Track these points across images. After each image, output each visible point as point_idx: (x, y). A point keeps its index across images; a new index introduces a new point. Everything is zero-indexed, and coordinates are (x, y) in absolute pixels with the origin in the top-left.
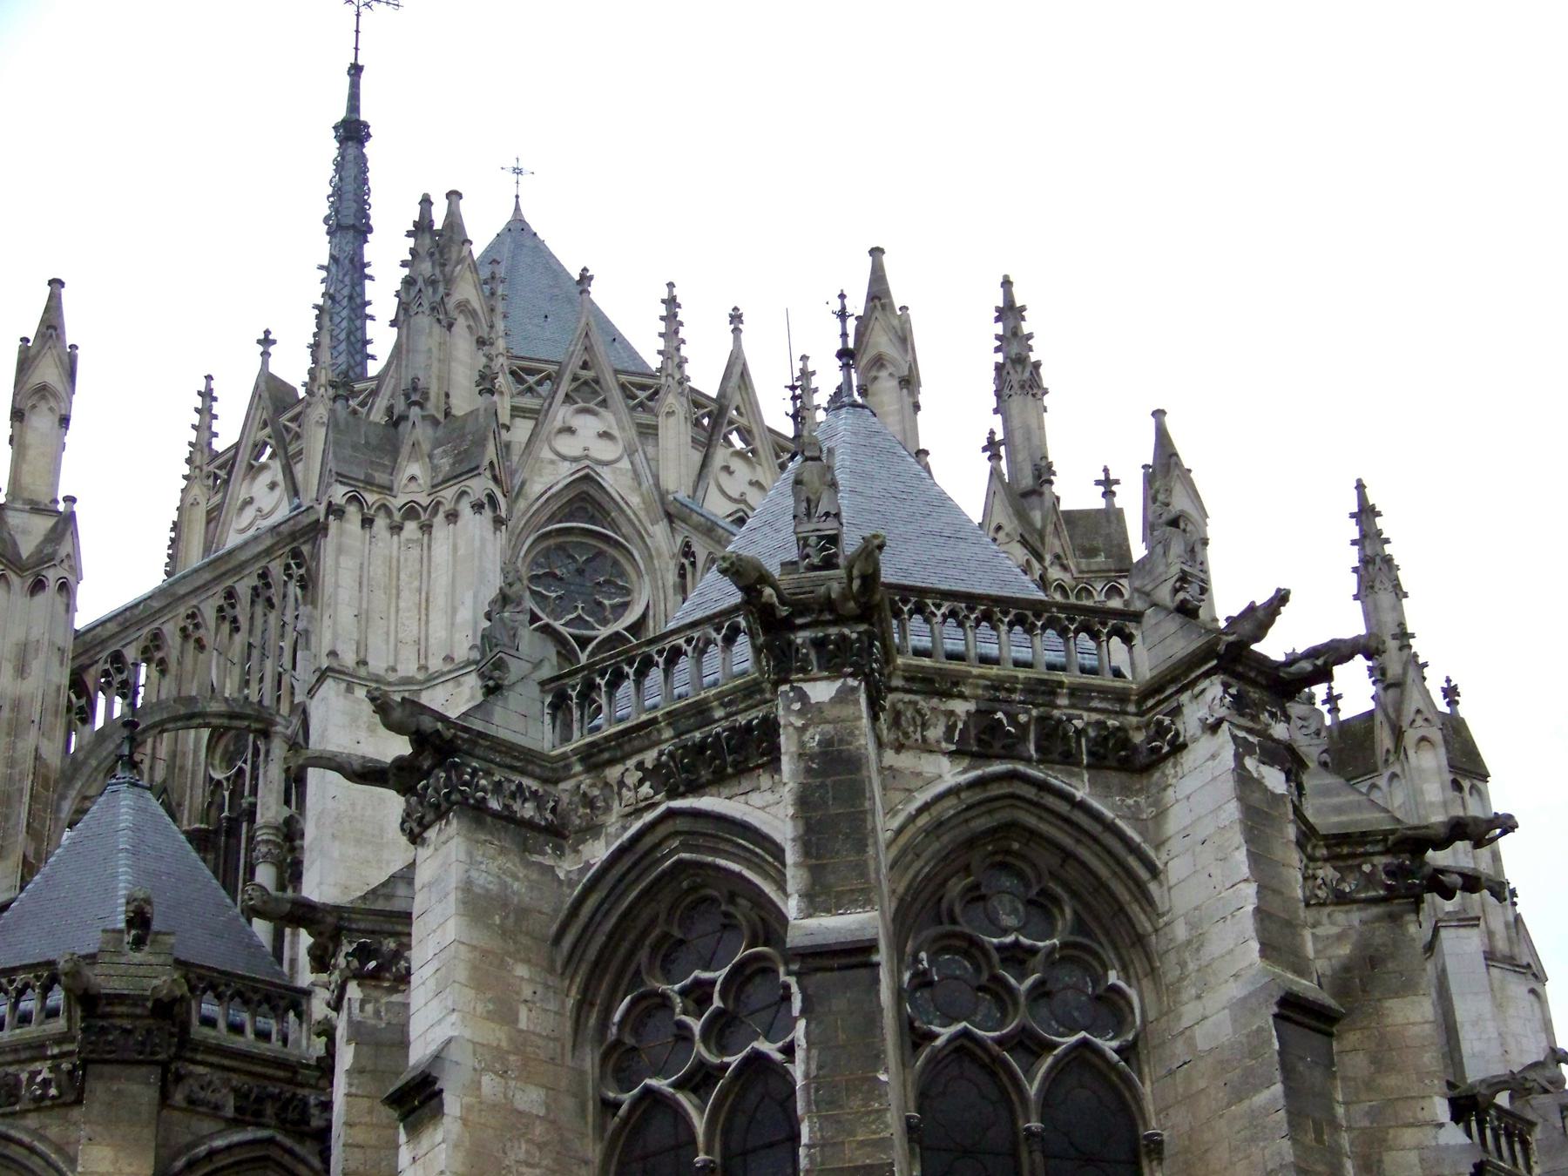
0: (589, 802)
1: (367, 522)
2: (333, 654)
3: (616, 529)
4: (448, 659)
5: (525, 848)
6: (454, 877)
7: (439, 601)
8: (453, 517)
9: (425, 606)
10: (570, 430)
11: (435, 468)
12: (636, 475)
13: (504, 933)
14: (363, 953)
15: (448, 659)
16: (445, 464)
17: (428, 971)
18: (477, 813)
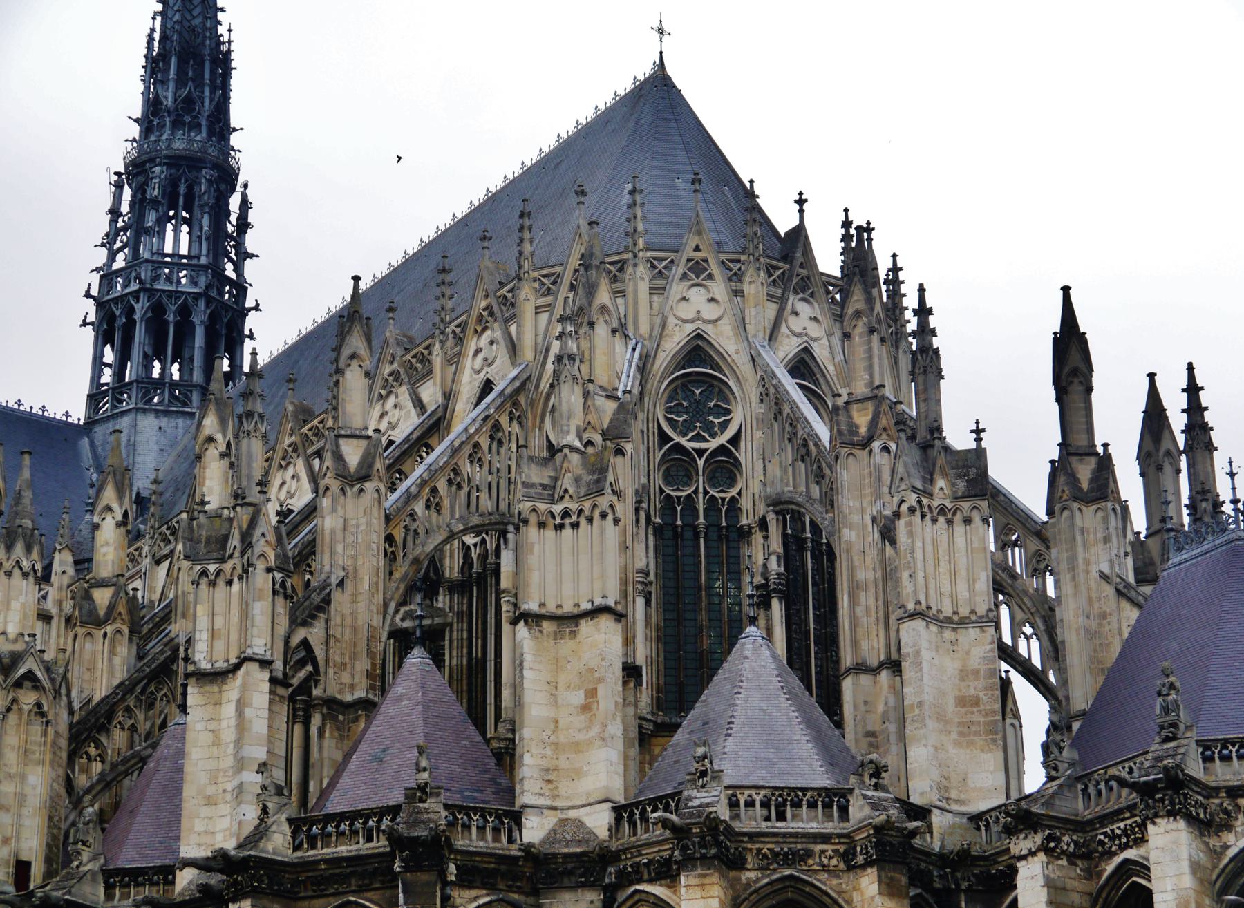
0: (1226, 812)
1: (923, 516)
2: (919, 603)
3: (816, 383)
5: (1202, 835)
6: (1185, 855)
7: (962, 573)
8: (967, 521)
9: (953, 574)
10: (796, 314)
11: (953, 485)
12: (831, 351)
13: (1201, 881)
14: (1050, 838)
15: (973, 612)
16: (961, 486)
17: (1169, 896)
18: (1192, 820)
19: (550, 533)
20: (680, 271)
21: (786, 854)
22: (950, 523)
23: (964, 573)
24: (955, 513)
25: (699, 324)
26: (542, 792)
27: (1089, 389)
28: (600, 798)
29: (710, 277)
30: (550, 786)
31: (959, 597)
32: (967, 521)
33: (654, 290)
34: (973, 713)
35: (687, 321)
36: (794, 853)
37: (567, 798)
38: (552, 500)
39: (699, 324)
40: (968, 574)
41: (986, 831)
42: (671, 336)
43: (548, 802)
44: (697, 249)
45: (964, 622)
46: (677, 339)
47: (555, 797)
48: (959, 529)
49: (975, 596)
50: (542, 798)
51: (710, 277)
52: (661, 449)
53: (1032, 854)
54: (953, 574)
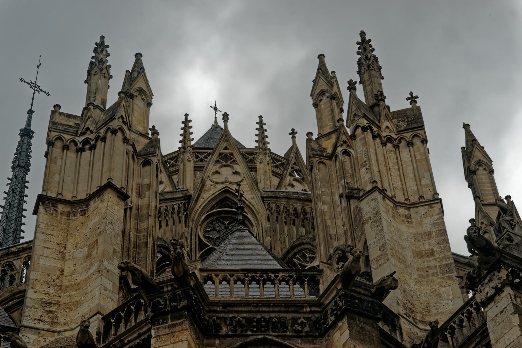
4: (421, 197)
9: (403, 177)
19: (71, 155)
20: (215, 157)
21: (259, 320)
22: (396, 147)
23: (411, 175)
24: (400, 142)
25: (227, 184)
26: (42, 318)
27: (492, 172)
28: (95, 313)
29: (235, 162)
30: (50, 315)
31: (409, 190)
32: (410, 144)
33: (196, 169)
34: (430, 261)
35: (218, 183)
36: (268, 321)
37: (65, 324)
38: (76, 134)
39: (227, 184)
40: (415, 176)
41: (452, 338)
42: (208, 191)
43: (47, 327)
44: (226, 148)
45: (415, 205)
46: (212, 192)
47: (53, 324)
48: (404, 150)
49: (422, 188)
50: (41, 323)
51: (235, 162)
52: (200, 252)
53: (499, 291)
54: (403, 177)
